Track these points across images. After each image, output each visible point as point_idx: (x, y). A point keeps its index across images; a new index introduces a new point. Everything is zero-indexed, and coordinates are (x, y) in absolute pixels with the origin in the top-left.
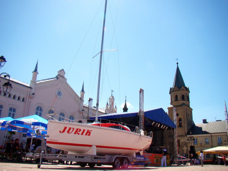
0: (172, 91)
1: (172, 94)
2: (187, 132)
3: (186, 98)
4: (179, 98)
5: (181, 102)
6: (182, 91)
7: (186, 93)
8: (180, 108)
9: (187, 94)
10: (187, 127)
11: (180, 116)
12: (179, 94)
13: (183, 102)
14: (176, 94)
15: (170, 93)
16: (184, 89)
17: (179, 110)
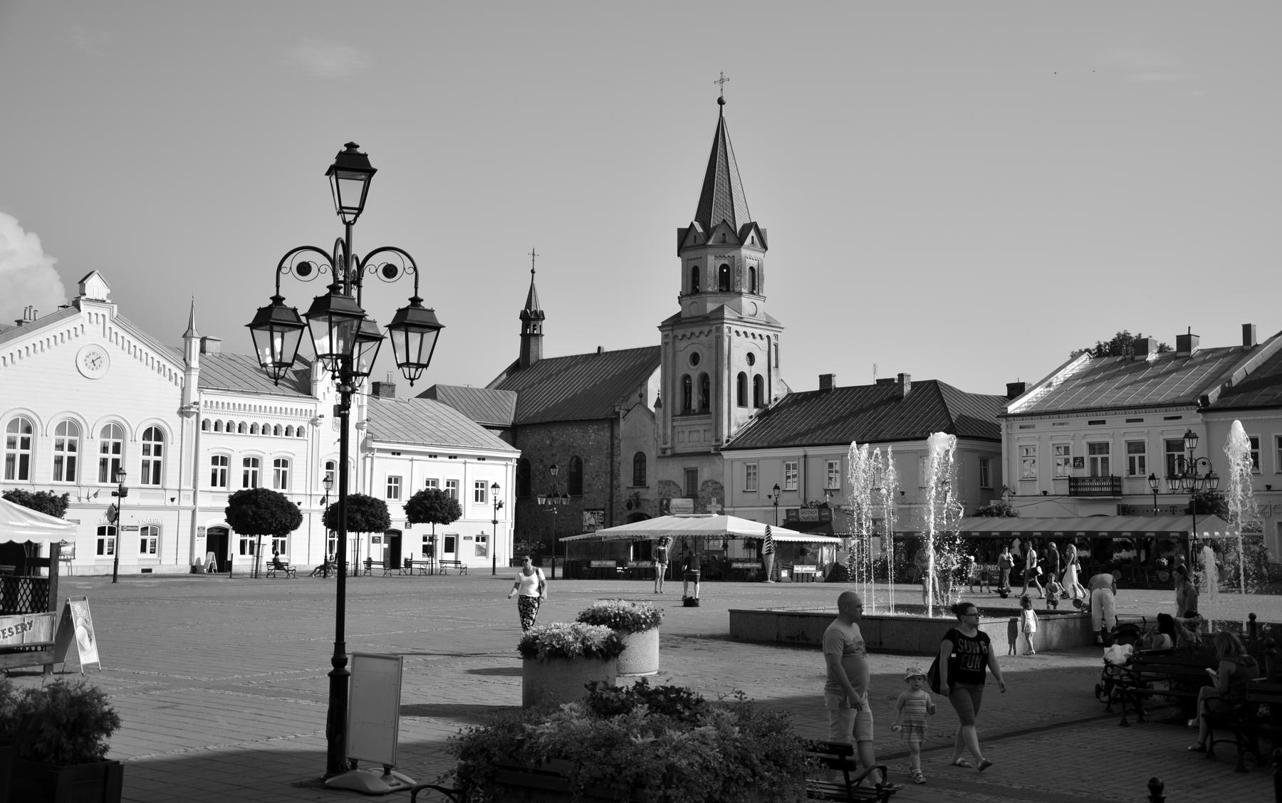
8: (706, 329)
11: (703, 367)
17: (702, 337)
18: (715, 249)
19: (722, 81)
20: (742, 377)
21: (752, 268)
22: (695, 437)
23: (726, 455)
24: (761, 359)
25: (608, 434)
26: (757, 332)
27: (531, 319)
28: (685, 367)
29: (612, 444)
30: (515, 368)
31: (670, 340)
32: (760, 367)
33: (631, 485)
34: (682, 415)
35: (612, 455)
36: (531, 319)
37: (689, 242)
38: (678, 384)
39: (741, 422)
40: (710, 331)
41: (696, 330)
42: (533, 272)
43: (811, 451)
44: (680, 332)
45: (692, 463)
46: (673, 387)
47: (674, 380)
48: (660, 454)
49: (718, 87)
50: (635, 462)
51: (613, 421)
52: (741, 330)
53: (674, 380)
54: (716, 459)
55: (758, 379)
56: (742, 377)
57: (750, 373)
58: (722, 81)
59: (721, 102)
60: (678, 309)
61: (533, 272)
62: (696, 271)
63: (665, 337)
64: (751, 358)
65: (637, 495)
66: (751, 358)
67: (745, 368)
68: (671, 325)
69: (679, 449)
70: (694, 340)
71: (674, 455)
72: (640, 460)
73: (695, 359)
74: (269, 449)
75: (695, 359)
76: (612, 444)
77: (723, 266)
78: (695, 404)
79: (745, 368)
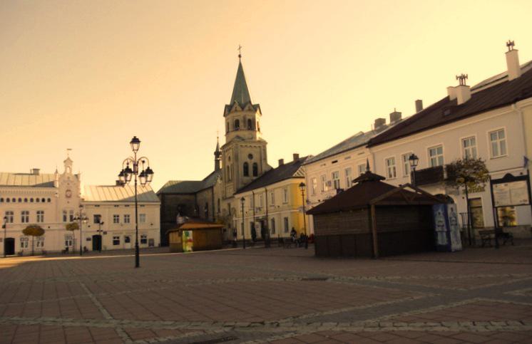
0: (229, 109)
1: (228, 117)
7: (242, 116)
8: (230, 146)
9: (244, 118)
16: (239, 108)
18: (241, 113)
19: (240, 48)
21: (249, 120)
32: (256, 159)
43: (255, 191)
46: (228, 171)
49: (238, 51)
52: (244, 145)
57: (251, 163)
58: (240, 48)
59: (240, 56)
64: (251, 156)
66: (251, 156)
71: (226, 199)
74: (33, 208)
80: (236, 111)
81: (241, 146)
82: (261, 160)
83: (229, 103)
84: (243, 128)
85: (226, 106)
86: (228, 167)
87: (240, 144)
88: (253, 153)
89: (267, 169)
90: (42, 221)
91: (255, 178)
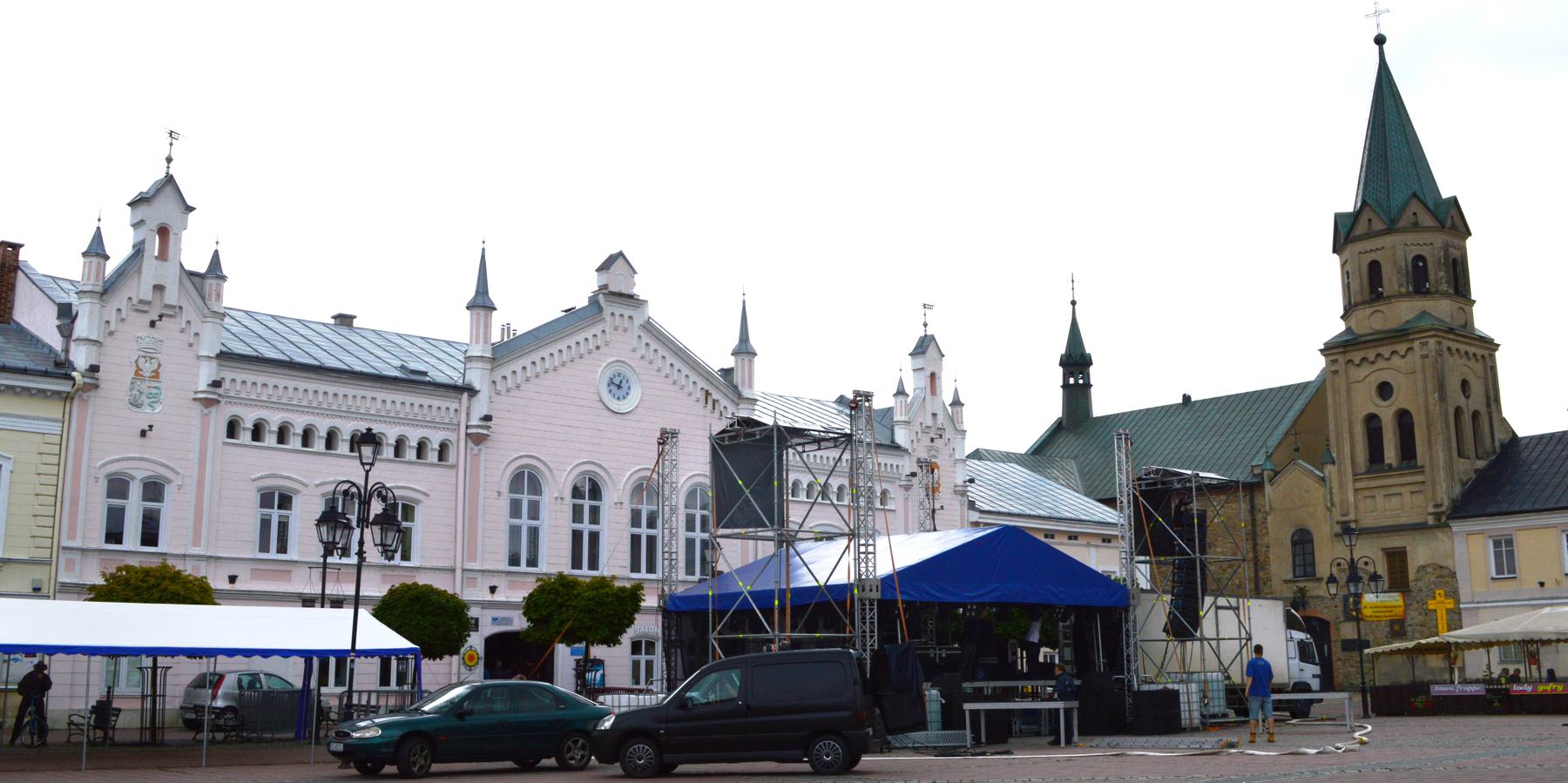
0: (1346, 232)
1: (1347, 254)
2: (1446, 503)
3: (1437, 275)
4: (1391, 280)
5: (1404, 311)
6: (1410, 238)
8: (1402, 348)
9: (1446, 248)
10: (1450, 466)
11: (1400, 400)
12: (1395, 250)
13: (1421, 304)
14: (1373, 256)
15: (1335, 251)
16: (1426, 220)
17: (1396, 360)
20: (1458, 411)
21: (1454, 261)
22: (1395, 501)
23: (1457, 527)
24: (1476, 387)
25: (1244, 506)
26: (1472, 350)
27: (1076, 362)
28: (1366, 402)
29: (1254, 520)
30: (1058, 429)
31: (1340, 367)
32: (1477, 401)
33: (1290, 576)
34: (1367, 472)
35: (1253, 535)
36: (1076, 362)
37: (1361, 228)
38: (1359, 429)
39: (1465, 479)
40: (1410, 349)
41: (1386, 351)
42: (1073, 303)
44: (1356, 356)
45: (1396, 542)
47: (1351, 423)
48: (1338, 529)
50: (1294, 544)
51: (1253, 488)
53: (1351, 423)
54: (1439, 534)
55: (1476, 415)
56: (1458, 411)
60: (1340, 327)
61: (1073, 303)
62: (1374, 267)
63: (1331, 362)
64: (1465, 384)
65: (1302, 591)
66: (1465, 384)
67: (1462, 401)
68: (1329, 350)
69: (1367, 521)
70: (1381, 364)
72: (1302, 541)
73: (1385, 390)
75: (1385, 390)
76: (1254, 520)
77: (1419, 258)
78: (1391, 454)
79: (1462, 401)
80: (1416, 227)
81: (1449, 349)
82: (1489, 405)
83: (1348, 207)
84: (1444, 287)
85: (1339, 218)
86: (1372, 422)
87: (1447, 343)
88: (1471, 378)
89: (1500, 436)
90: (282, 549)
91: (1481, 464)
